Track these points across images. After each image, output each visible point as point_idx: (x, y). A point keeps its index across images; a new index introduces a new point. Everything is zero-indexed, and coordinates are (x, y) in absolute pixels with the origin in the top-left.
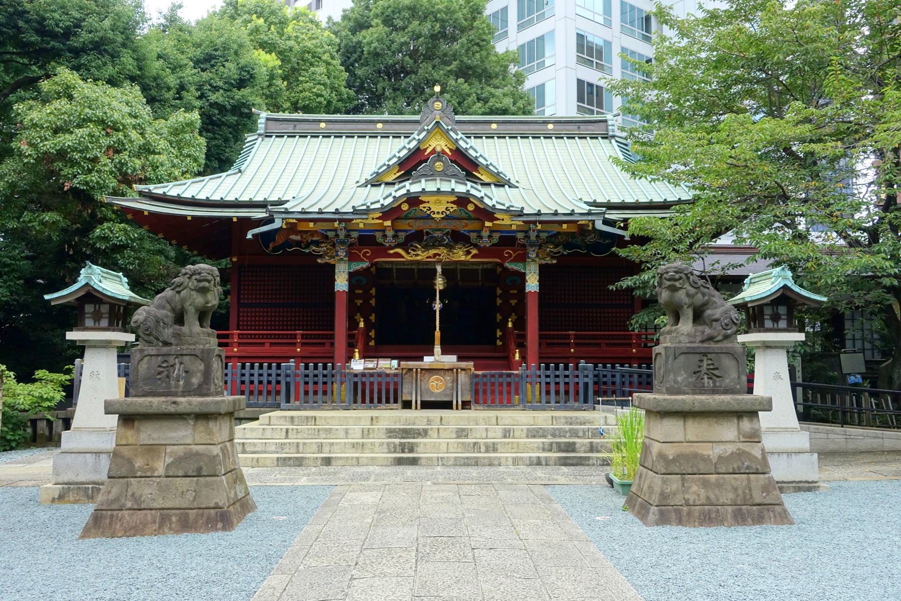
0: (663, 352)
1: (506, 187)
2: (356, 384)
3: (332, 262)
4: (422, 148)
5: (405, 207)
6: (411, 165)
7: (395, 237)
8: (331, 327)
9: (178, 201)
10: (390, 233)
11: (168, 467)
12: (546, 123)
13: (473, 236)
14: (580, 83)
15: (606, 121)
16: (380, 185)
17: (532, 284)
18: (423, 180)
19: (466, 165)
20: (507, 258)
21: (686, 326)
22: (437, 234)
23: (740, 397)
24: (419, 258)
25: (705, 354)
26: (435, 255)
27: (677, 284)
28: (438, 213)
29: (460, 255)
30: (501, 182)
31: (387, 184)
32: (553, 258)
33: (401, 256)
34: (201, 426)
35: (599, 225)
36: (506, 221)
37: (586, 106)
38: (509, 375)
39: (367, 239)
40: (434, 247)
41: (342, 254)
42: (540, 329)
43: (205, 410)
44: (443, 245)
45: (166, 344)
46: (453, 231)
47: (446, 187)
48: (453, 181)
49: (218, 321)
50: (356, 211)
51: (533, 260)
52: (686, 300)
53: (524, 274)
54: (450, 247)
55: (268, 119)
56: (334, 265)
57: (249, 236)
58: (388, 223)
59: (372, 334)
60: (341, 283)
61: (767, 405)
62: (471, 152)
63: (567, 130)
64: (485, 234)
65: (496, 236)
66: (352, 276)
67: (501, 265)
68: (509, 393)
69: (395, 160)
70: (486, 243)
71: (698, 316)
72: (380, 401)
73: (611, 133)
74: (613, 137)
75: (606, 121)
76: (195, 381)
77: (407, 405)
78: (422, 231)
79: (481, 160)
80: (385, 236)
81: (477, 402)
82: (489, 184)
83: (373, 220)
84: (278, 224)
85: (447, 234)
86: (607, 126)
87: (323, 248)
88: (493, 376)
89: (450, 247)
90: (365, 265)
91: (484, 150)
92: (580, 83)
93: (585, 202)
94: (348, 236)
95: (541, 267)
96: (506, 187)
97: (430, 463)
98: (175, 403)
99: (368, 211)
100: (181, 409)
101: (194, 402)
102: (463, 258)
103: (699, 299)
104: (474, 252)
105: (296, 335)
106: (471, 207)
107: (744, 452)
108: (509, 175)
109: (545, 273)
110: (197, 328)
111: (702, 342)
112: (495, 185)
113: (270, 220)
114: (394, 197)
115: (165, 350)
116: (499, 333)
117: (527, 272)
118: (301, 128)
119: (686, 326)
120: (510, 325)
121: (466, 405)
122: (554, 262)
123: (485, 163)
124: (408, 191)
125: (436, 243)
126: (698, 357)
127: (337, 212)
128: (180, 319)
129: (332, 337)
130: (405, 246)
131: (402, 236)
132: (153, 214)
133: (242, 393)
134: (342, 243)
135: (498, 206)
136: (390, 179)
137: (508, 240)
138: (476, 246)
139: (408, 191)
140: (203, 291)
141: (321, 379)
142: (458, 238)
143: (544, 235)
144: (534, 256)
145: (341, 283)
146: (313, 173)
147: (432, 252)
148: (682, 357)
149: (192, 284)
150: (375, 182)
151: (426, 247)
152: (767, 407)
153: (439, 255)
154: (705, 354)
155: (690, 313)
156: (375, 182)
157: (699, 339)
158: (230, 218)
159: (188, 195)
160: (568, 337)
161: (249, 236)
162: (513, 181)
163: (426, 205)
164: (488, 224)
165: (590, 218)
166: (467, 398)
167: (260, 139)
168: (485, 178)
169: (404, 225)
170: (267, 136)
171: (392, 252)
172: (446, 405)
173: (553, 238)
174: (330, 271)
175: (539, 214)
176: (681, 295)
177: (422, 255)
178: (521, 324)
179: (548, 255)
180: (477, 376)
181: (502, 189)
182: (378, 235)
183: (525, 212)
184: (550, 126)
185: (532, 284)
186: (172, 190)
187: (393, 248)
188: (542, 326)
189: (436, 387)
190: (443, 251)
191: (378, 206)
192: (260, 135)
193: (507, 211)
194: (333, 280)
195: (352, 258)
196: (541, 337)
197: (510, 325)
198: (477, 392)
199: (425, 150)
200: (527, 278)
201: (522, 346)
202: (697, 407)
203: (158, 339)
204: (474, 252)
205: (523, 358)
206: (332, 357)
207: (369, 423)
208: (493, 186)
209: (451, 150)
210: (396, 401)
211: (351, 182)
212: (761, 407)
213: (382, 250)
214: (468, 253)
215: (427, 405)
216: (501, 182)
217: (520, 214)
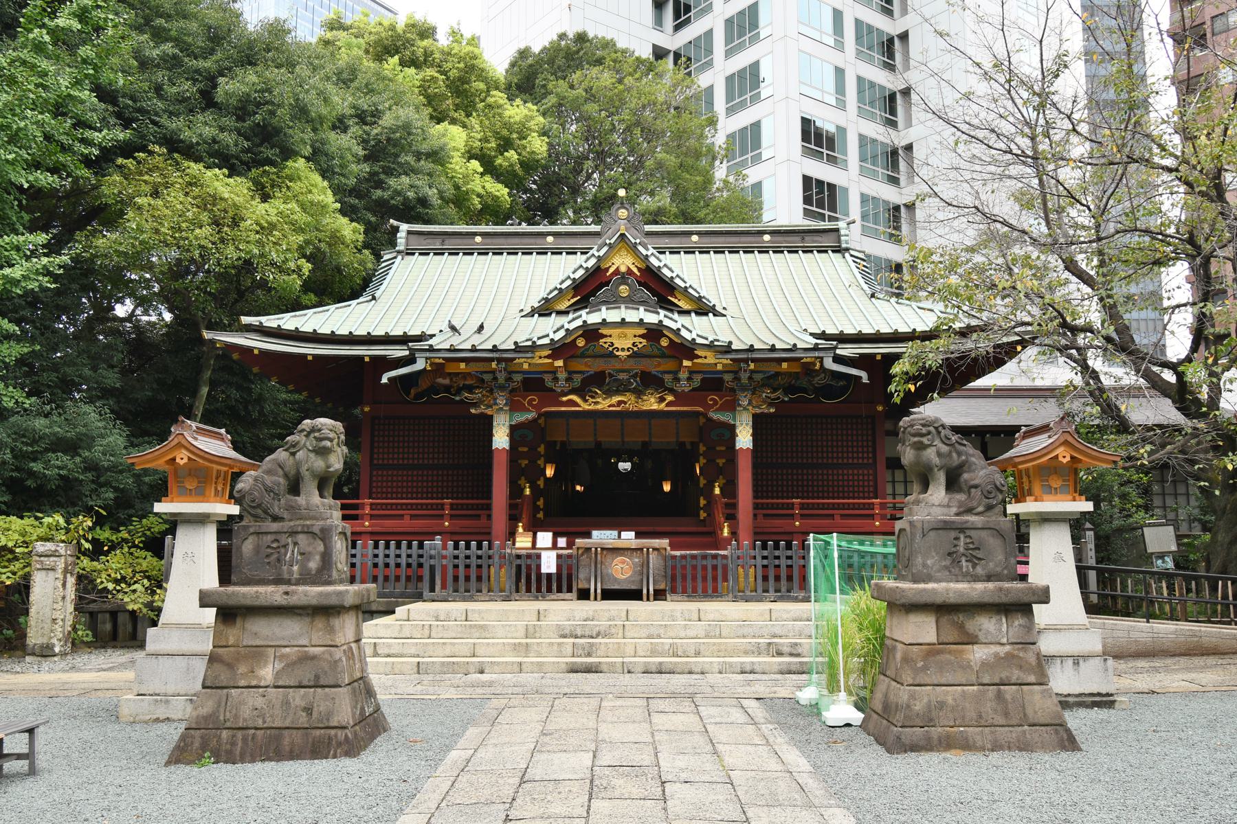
0: (908, 529)
1: (711, 315)
2: (519, 567)
3: (489, 412)
4: (603, 266)
5: (581, 343)
6: (588, 289)
7: (568, 380)
8: (488, 494)
9: (296, 336)
10: (562, 375)
11: (277, 675)
12: (764, 232)
13: (668, 378)
14: (807, 180)
15: (837, 230)
16: (550, 314)
17: (744, 439)
18: (604, 308)
19: (660, 289)
20: (712, 406)
21: (938, 492)
22: (623, 376)
23: (1007, 585)
24: (599, 407)
25: (962, 530)
26: (620, 403)
27: (925, 440)
28: (623, 349)
29: (651, 403)
30: (703, 309)
31: (559, 313)
32: (770, 405)
33: (577, 405)
34: (320, 623)
35: (829, 364)
36: (710, 358)
37: (814, 209)
38: (715, 557)
39: (534, 384)
40: (618, 392)
41: (501, 401)
42: (755, 497)
43: (325, 602)
44: (629, 391)
45: (276, 519)
46: (642, 372)
47: (632, 316)
48: (642, 309)
49: (343, 488)
50: (518, 348)
51: (745, 409)
52: (936, 460)
53: (734, 426)
54: (639, 393)
55: (409, 233)
56: (492, 416)
57: (384, 380)
58: (559, 363)
59: (541, 503)
60: (501, 440)
61: (1044, 596)
62: (665, 271)
63: (789, 241)
64: (683, 375)
65: (698, 378)
66: (513, 429)
67: (705, 415)
68: (715, 579)
69: (569, 282)
70: (684, 386)
71: (952, 484)
72: (549, 590)
73: (844, 246)
74: (847, 250)
75: (837, 230)
76: (313, 565)
77: (584, 595)
78: (603, 373)
79: (677, 281)
80: (556, 379)
81: (674, 591)
82: (688, 312)
83: (541, 360)
84: (420, 365)
85: (634, 376)
86: (839, 236)
87: (477, 395)
88: (694, 557)
90: (530, 416)
91: (684, 269)
92: (807, 180)
93: (811, 334)
94: (509, 379)
95: (755, 416)
96: (711, 315)
97: (612, 668)
98: (287, 593)
99: (534, 347)
100: (293, 600)
101: (311, 593)
102: (655, 407)
103: (955, 460)
104: (670, 398)
105: (443, 504)
106: (664, 343)
107: (1013, 656)
108: (713, 299)
109: (759, 424)
110: (316, 499)
111: (957, 514)
112: (697, 314)
113: (411, 360)
114: (567, 330)
115: (275, 526)
116: (702, 502)
117: (738, 423)
118: (450, 244)
119: (938, 492)
120: (717, 491)
121: (659, 595)
122: (772, 410)
123: (683, 285)
124: (585, 322)
125: (621, 388)
126: (953, 534)
127: (495, 349)
128: (294, 487)
129: (488, 507)
130: (582, 391)
131: (578, 378)
132: (264, 353)
133: (375, 579)
134: (502, 388)
135: (699, 341)
136: (563, 306)
137: (712, 383)
138: (671, 391)
139: (585, 322)
140: (322, 452)
141: (474, 562)
142: (649, 382)
143: (758, 377)
144: (746, 403)
145: (501, 440)
146: (463, 299)
147: (616, 399)
148: (932, 533)
150: (544, 309)
151: (609, 393)
152: (1044, 599)
153: (625, 403)
154: (962, 530)
155: (941, 477)
156: (544, 309)
157: (954, 510)
158: (361, 358)
159: (307, 328)
160: (792, 506)
161: (384, 380)
162: (719, 308)
163: (608, 340)
164: (686, 363)
165: (817, 354)
166: (662, 587)
167: (400, 257)
168: (684, 305)
169: (579, 365)
170: (408, 254)
171: (565, 399)
172: (634, 595)
173: (771, 381)
174: (486, 424)
175: (751, 349)
176: (930, 454)
178: (730, 489)
179: (764, 402)
180: (674, 557)
181: (704, 318)
182: (548, 378)
183: (734, 347)
184: (767, 237)
185: (744, 439)
186: (289, 321)
187: (566, 395)
188: (758, 491)
189: (621, 571)
191: (546, 341)
192: (399, 252)
193: (711, 346)
194: (491, 435)
195: (514, 407)
196: (756, 507)
197: (717, 491)
198: (674, 578)
199: (607, 269)
200: (737, 431)
201: (731, 518)
202: (952, 599)
203: (265, 512)
204: (670, 398)
205: (734, 533)
206: (489, 533)
207: (535, 618)
208: (693, 314)
209: (639, 269)
210: (570, 590)
211: (514, 311)
212: (1036, 598)
213: (552, 396)
214: (662, 400)
215: (610, 595)
216: (703, 309)
217: (727, 349)
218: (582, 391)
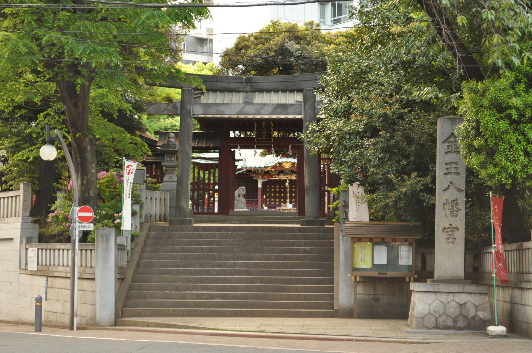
5: (278, 165)
22: (287, 171)
41: (260, 177)
49: (245, 196)
50: (265, 167)
58: (273, 170)
60: (260, 185)
66: (263, 184)
84: (244, 170)
87: (254, 175)
89: (291, 175)
99: (268, 167)
125: (286, 174)
129: (257, 201)
131: (277, 172)
134: (260, 174)
145: (260, 185)
149: (241, 190)
151: (284, 175)
174: (256, 182)
177: (282, 177)
190: (289, 176)
191: (270, 165)
195: (263, 178)
218: (278, 174)
